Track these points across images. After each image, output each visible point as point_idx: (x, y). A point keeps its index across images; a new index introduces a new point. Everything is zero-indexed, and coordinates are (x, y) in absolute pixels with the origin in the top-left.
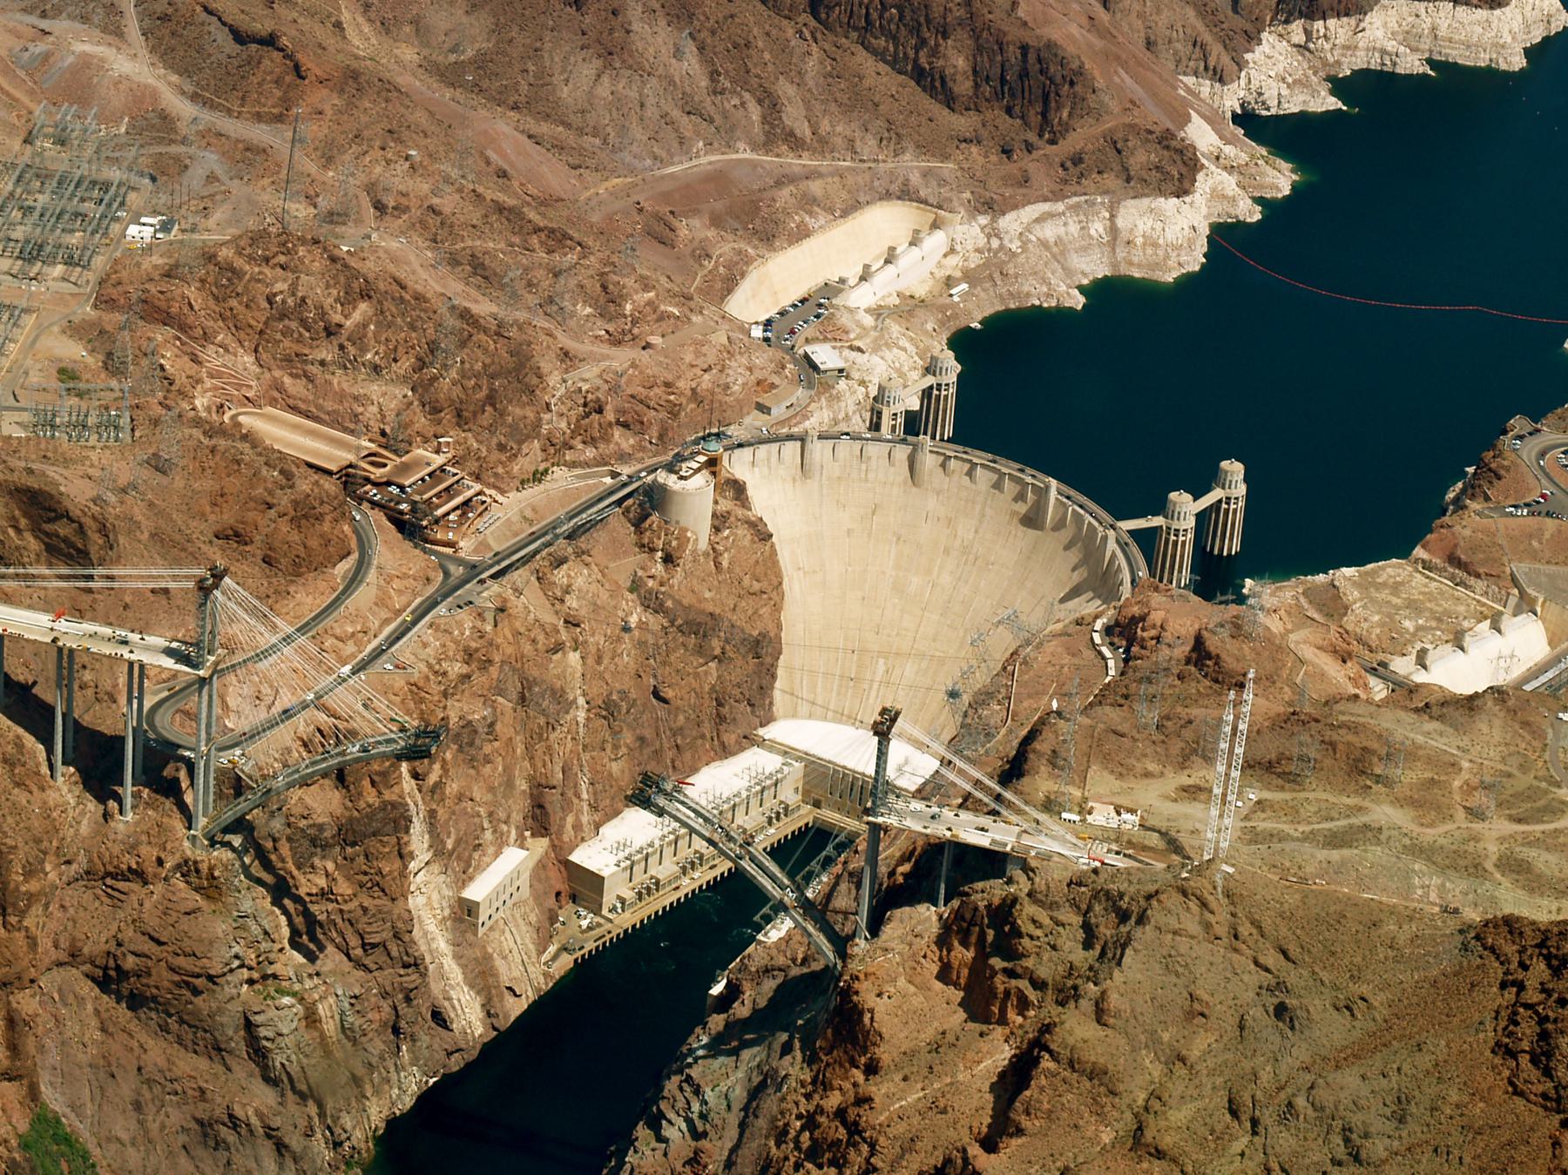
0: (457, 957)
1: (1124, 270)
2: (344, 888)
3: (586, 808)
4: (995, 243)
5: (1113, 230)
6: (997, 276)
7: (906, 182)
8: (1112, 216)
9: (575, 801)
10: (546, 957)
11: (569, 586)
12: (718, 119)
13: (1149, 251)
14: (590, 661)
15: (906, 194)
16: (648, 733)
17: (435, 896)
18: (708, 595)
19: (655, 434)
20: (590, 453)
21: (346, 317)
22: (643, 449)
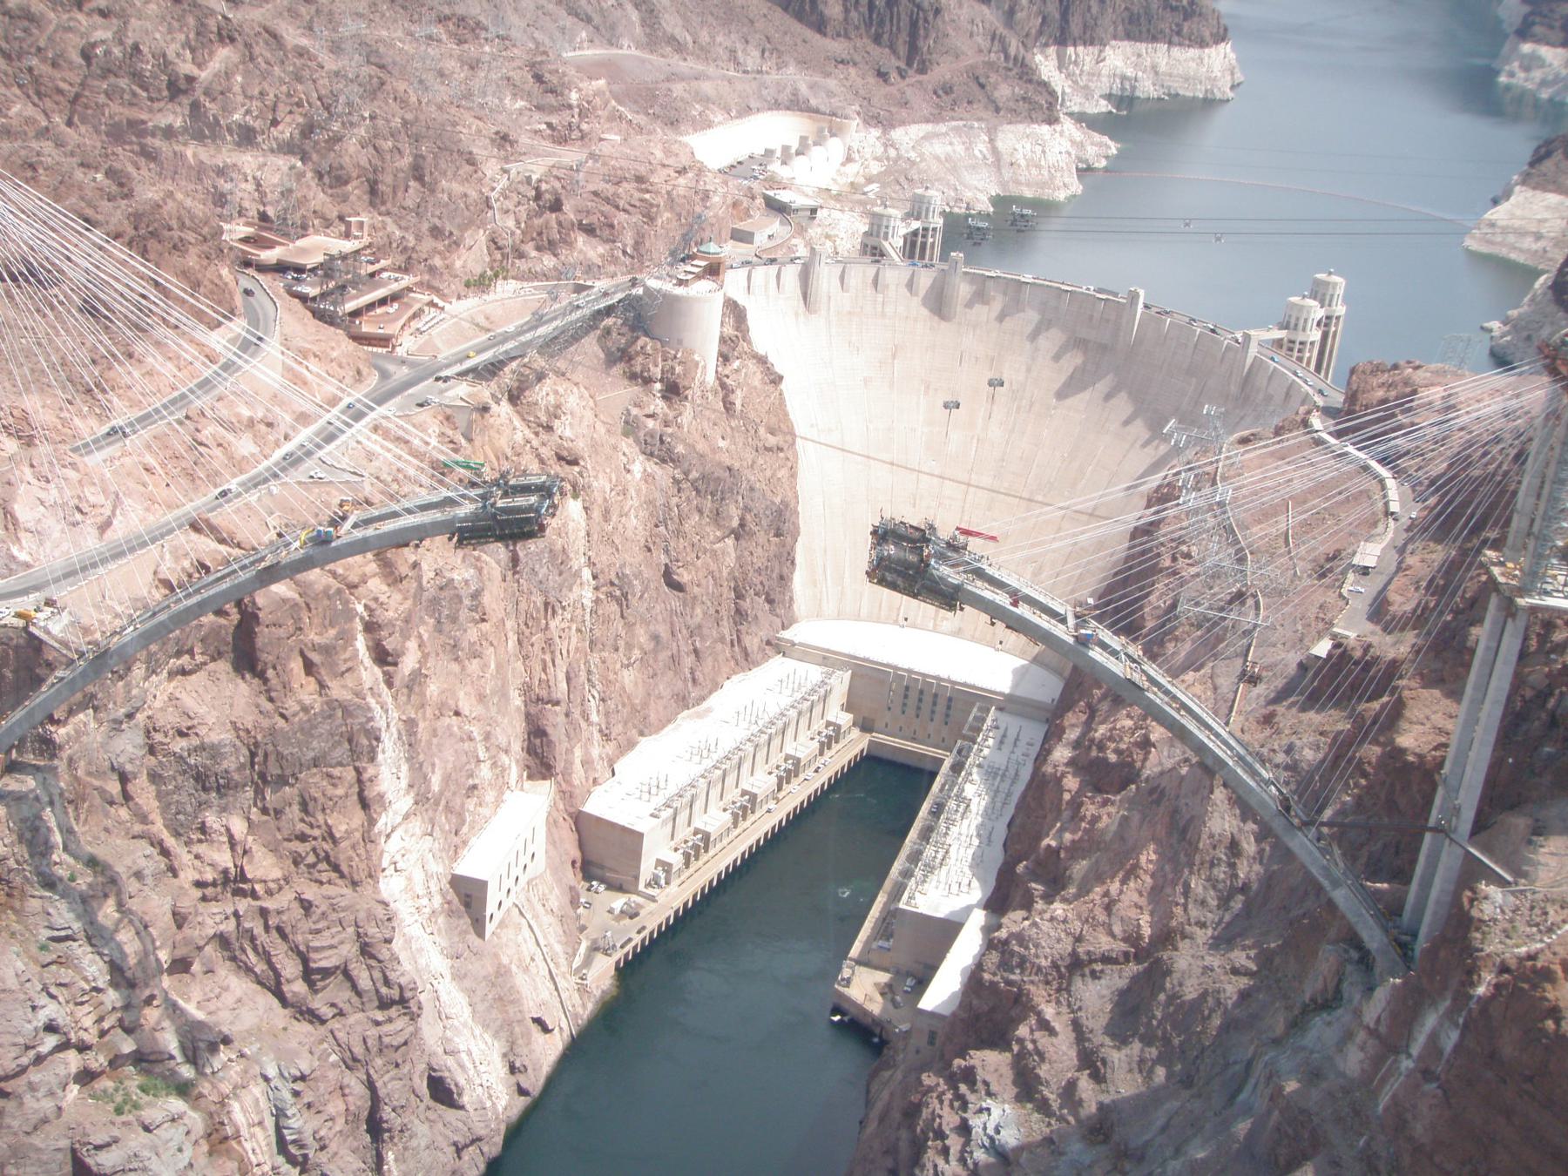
0: (458, 976)
1: (1014, 190)
2: (264, 867)
3: (597, 736)
4: (892, 153)
5: (995, 151)
6: (902, 180)
7: (795, 93)
8: (991, 141)
9: (584, 725)
10: (577, 962)
11: (558, 406)
12: (597, 19)
13: (1034, 171)
14: (596, 514)
15: (796, 104)
16: (663, 630)
17: (419, 876)
18: (722, 443)
19: (630, 241)
20: (549, 261)
21: (200, 66)
22: (614, 260)
